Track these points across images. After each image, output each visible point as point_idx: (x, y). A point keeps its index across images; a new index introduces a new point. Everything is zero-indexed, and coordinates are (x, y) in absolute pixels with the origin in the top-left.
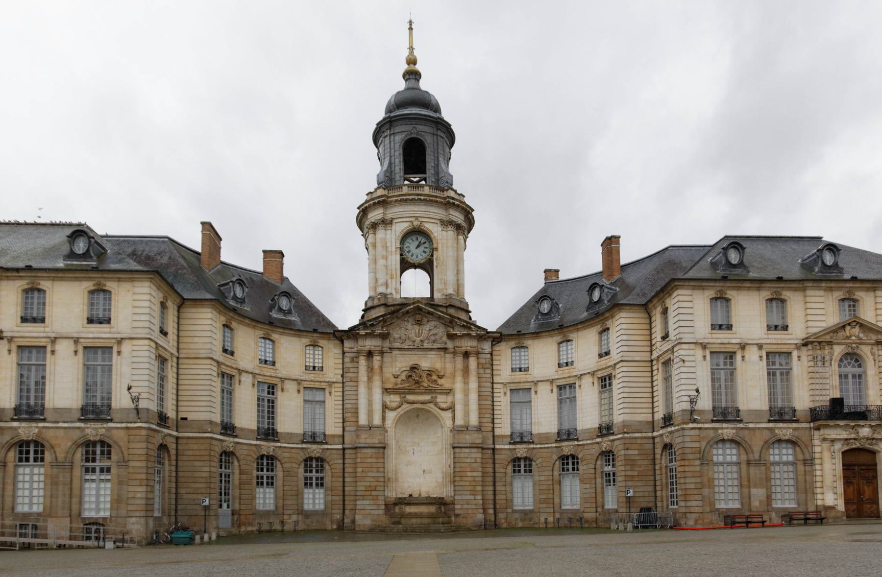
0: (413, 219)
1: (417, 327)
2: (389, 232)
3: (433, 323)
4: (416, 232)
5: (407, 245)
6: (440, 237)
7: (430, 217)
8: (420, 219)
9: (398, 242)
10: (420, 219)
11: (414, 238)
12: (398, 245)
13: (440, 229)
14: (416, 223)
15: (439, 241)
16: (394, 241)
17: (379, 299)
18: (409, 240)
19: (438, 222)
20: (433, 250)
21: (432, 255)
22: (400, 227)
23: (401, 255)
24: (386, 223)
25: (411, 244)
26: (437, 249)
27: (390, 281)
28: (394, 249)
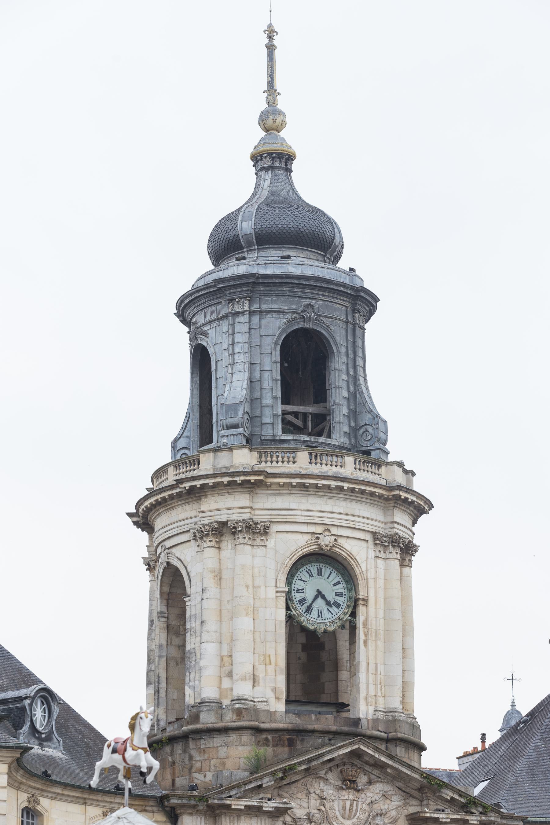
0: (319, 529)
1: (348, 795)
2: (260, 552)
3: (379, 788)
4: (324, 558)
5: (298, 584)
6: (371, 575)
7: (351, 525)
8: (334, 531)
9: (283, 578)
10: (334, 531)
11: (314, 571)
12: (283, 586)
13: (372, 554)
14: (326, 541)
15: (371, 583)
16: (271, 575)
17: (239, 713)
18: (303, 574)
19: (369, 537)
20: (355, 604)
21: (353, 614)
22: (289, 544)
23: (288, 608)
24: (256, 530)
25: (309, 584)
26: (366, 600)
27: (261, 671)
28: (271, 593)
